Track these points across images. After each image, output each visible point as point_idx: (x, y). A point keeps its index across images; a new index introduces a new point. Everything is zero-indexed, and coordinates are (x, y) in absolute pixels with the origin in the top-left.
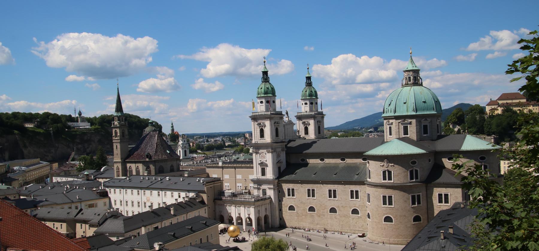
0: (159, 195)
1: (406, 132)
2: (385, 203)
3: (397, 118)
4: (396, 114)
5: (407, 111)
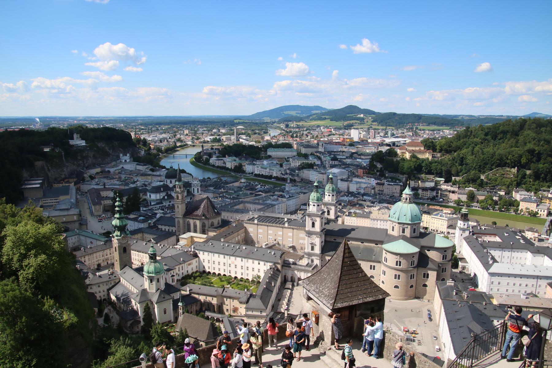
1: (403, 232)
2: (395, 278)
3: (399, 223)
4: (399, 221)
5: (406, 220)
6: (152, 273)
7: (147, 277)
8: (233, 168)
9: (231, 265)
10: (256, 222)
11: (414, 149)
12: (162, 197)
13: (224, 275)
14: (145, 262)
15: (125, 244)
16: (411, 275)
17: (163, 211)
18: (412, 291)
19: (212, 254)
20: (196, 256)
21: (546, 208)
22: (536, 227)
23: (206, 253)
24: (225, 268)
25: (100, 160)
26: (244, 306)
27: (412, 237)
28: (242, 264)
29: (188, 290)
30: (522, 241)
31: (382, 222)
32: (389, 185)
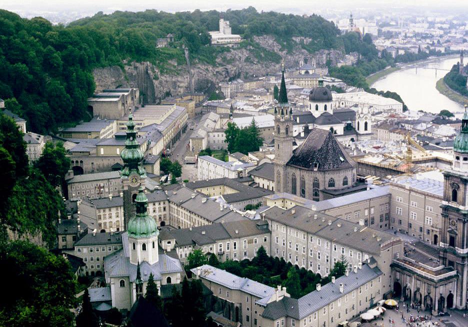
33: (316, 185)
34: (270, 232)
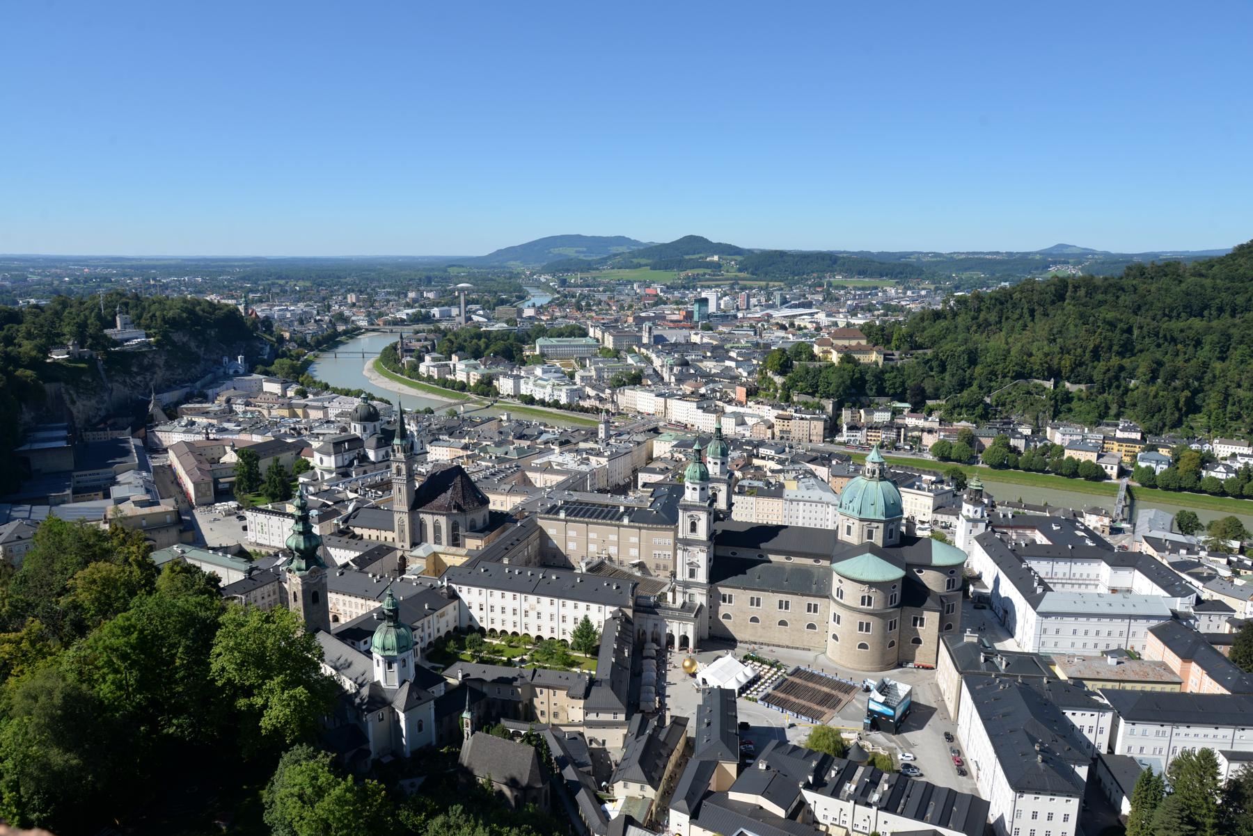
0: (552, 604)
1: (870, 535)
2: (861, 629)
3: (861, 520)
4: (862, 516)
5: (875, 514)
6: (393, 649)
7: (380, 658)
8: (472, 384)
9: (530, 613)
10: (562, 515)
11: (846, 343)
12: (347, 462)
13: (515, 634)
14: (341, 612)
15: (315, 584)
16: (891, 623)
17: (356, 495)
18: (893, 654)
19: (489, 591)
20: (454, 596)
21: (1116, 461)
22: (1104, 502)
23: (475, 590)
24: (517, 618)
25: (180, 371)
26: (581, 703)
27: (886, 546)
28: (554, 609)
29: (460, 676)
30: (1089, 543)
31: (808, 504)
32: (802, 419)
33: (454, 528)
34: (459, 598)
